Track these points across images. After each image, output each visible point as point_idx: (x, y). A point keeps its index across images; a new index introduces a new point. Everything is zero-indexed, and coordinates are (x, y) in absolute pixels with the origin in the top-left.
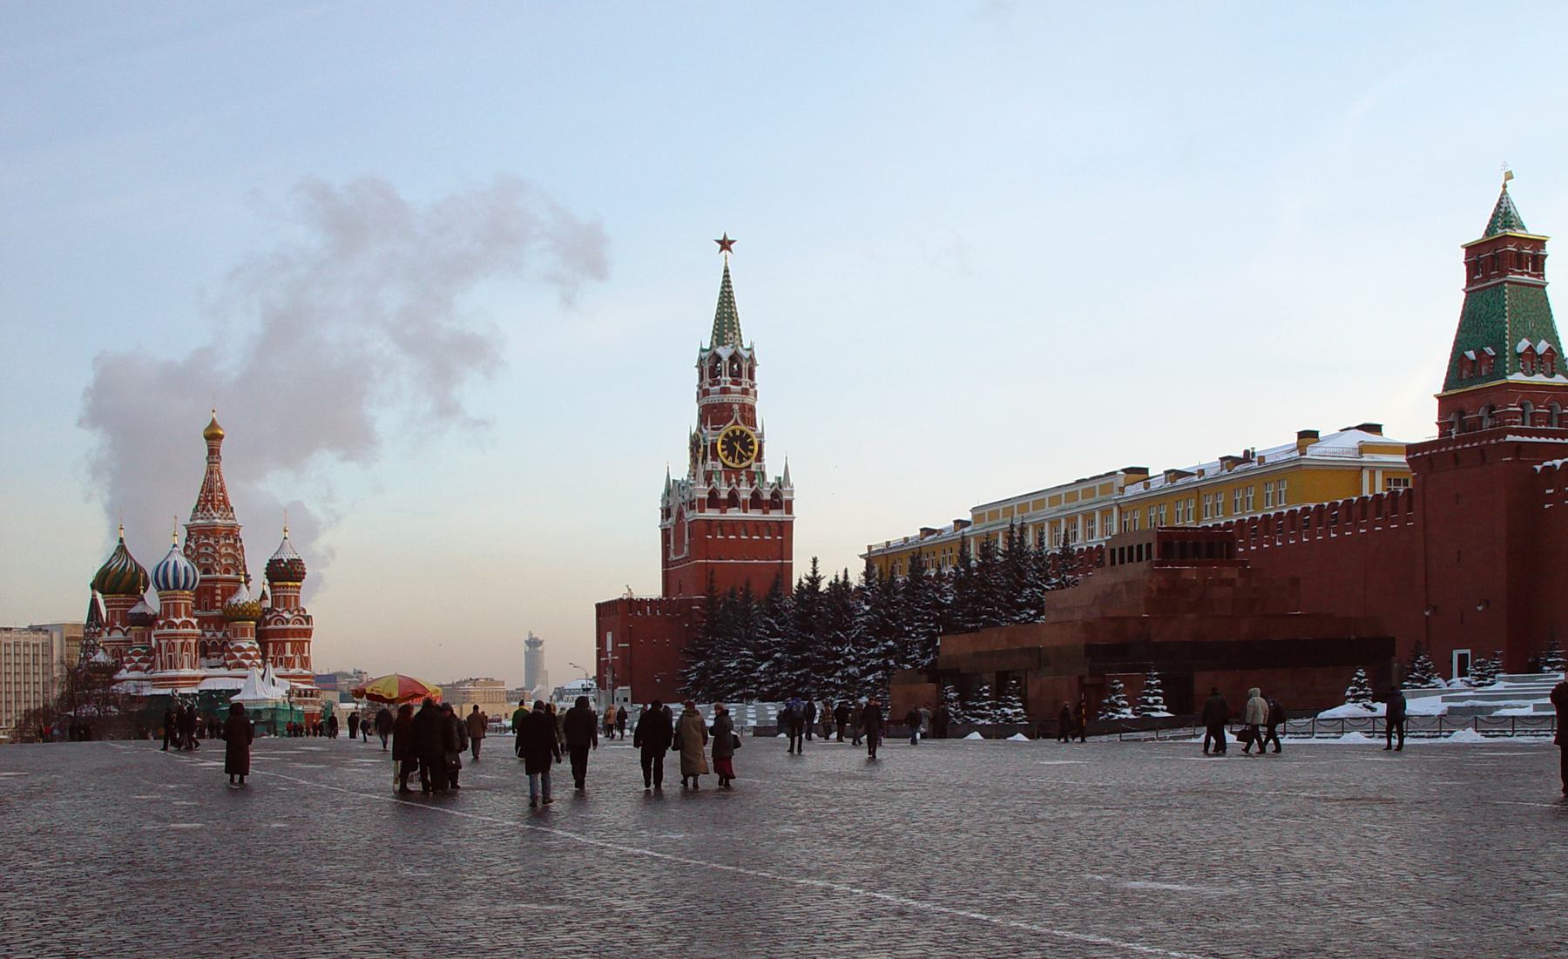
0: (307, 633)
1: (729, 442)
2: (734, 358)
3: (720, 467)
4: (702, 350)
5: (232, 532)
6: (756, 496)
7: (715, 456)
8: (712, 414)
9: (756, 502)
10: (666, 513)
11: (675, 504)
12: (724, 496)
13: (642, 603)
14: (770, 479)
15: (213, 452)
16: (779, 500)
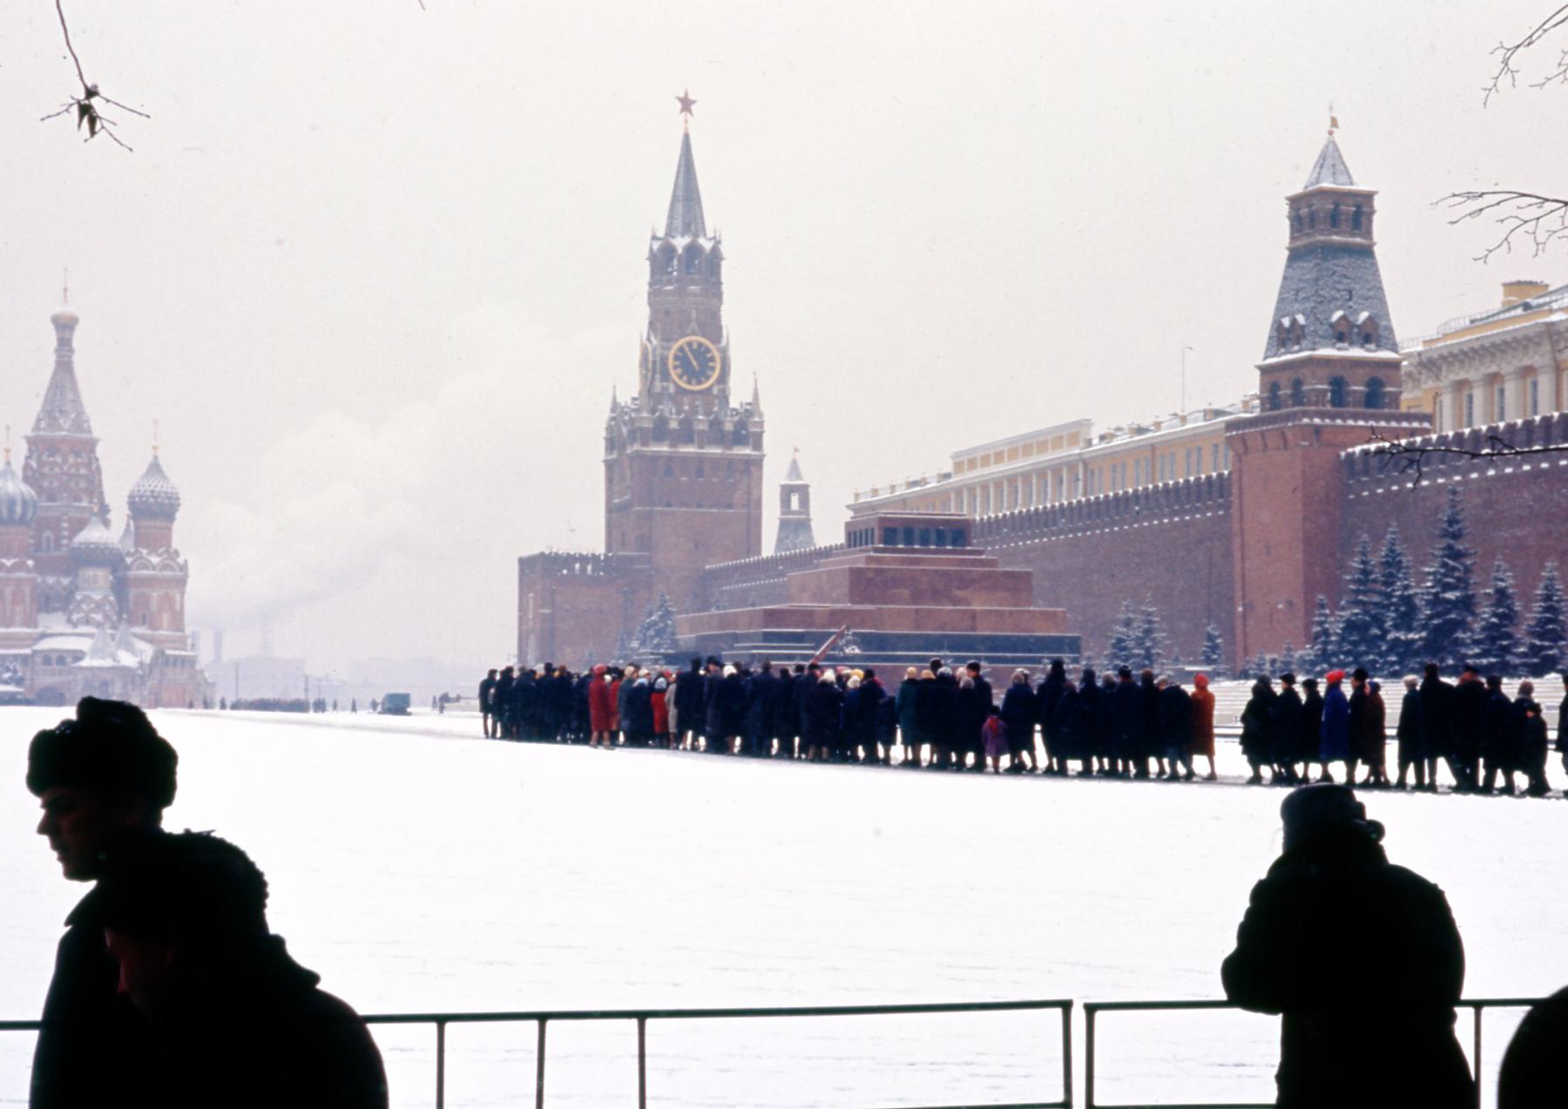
0: (181, 582)
1: (682, 358)
2: (693, 250)
3: (672, 389)
4: (654, 238)
5: (86, 448)
6: (716, 424)
7: (666, 376)
8: (664, 320)
9: (716, 434)
10: (612, 443)
11: (622, 435)
12: (674, 425)
13: (569, 560)
14: (734, 403)
15: (65, 345)
16: (746, 430)
